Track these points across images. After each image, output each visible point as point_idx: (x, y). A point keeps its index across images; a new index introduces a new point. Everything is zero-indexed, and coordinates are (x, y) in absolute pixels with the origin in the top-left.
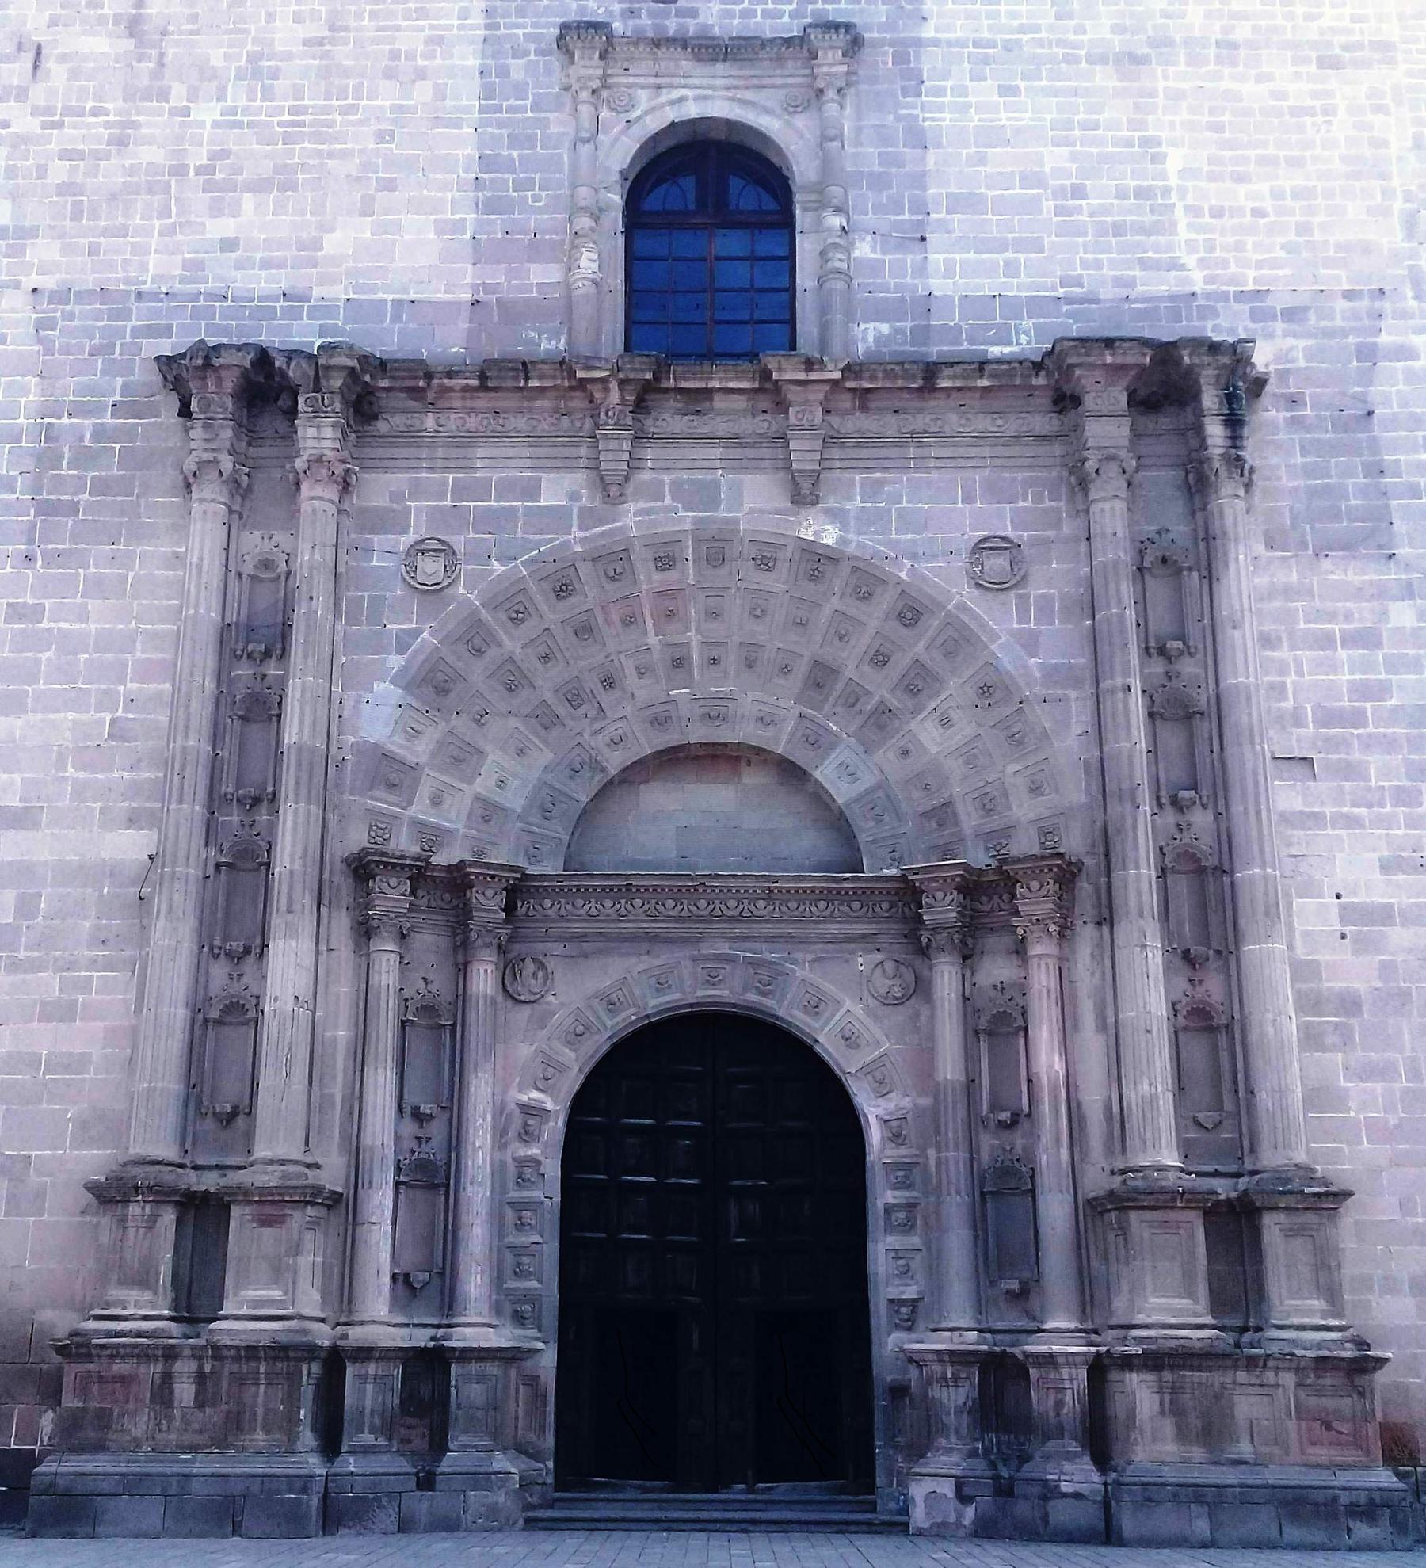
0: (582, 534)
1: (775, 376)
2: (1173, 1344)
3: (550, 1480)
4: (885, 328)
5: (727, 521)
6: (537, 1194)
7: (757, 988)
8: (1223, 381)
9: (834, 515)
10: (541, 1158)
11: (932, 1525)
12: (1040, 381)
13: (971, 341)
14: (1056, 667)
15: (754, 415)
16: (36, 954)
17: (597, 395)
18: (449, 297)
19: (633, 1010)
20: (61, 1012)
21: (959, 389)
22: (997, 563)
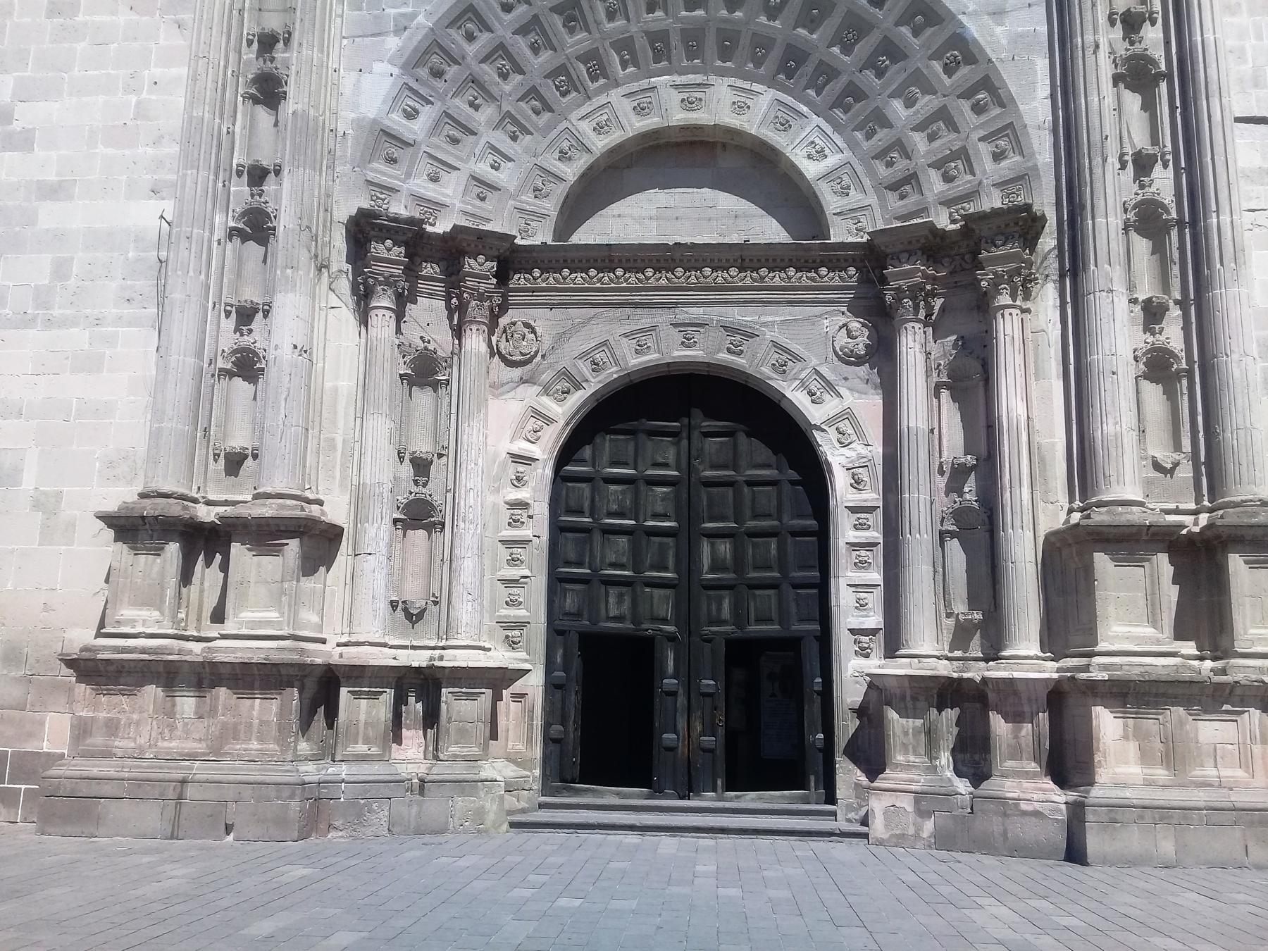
2: (1137, 671)
3: (537, 786)
6: (525, 532)
14: (1021, 35)
16: (68, 312)
19: (615, 369)
20: (89, 364)
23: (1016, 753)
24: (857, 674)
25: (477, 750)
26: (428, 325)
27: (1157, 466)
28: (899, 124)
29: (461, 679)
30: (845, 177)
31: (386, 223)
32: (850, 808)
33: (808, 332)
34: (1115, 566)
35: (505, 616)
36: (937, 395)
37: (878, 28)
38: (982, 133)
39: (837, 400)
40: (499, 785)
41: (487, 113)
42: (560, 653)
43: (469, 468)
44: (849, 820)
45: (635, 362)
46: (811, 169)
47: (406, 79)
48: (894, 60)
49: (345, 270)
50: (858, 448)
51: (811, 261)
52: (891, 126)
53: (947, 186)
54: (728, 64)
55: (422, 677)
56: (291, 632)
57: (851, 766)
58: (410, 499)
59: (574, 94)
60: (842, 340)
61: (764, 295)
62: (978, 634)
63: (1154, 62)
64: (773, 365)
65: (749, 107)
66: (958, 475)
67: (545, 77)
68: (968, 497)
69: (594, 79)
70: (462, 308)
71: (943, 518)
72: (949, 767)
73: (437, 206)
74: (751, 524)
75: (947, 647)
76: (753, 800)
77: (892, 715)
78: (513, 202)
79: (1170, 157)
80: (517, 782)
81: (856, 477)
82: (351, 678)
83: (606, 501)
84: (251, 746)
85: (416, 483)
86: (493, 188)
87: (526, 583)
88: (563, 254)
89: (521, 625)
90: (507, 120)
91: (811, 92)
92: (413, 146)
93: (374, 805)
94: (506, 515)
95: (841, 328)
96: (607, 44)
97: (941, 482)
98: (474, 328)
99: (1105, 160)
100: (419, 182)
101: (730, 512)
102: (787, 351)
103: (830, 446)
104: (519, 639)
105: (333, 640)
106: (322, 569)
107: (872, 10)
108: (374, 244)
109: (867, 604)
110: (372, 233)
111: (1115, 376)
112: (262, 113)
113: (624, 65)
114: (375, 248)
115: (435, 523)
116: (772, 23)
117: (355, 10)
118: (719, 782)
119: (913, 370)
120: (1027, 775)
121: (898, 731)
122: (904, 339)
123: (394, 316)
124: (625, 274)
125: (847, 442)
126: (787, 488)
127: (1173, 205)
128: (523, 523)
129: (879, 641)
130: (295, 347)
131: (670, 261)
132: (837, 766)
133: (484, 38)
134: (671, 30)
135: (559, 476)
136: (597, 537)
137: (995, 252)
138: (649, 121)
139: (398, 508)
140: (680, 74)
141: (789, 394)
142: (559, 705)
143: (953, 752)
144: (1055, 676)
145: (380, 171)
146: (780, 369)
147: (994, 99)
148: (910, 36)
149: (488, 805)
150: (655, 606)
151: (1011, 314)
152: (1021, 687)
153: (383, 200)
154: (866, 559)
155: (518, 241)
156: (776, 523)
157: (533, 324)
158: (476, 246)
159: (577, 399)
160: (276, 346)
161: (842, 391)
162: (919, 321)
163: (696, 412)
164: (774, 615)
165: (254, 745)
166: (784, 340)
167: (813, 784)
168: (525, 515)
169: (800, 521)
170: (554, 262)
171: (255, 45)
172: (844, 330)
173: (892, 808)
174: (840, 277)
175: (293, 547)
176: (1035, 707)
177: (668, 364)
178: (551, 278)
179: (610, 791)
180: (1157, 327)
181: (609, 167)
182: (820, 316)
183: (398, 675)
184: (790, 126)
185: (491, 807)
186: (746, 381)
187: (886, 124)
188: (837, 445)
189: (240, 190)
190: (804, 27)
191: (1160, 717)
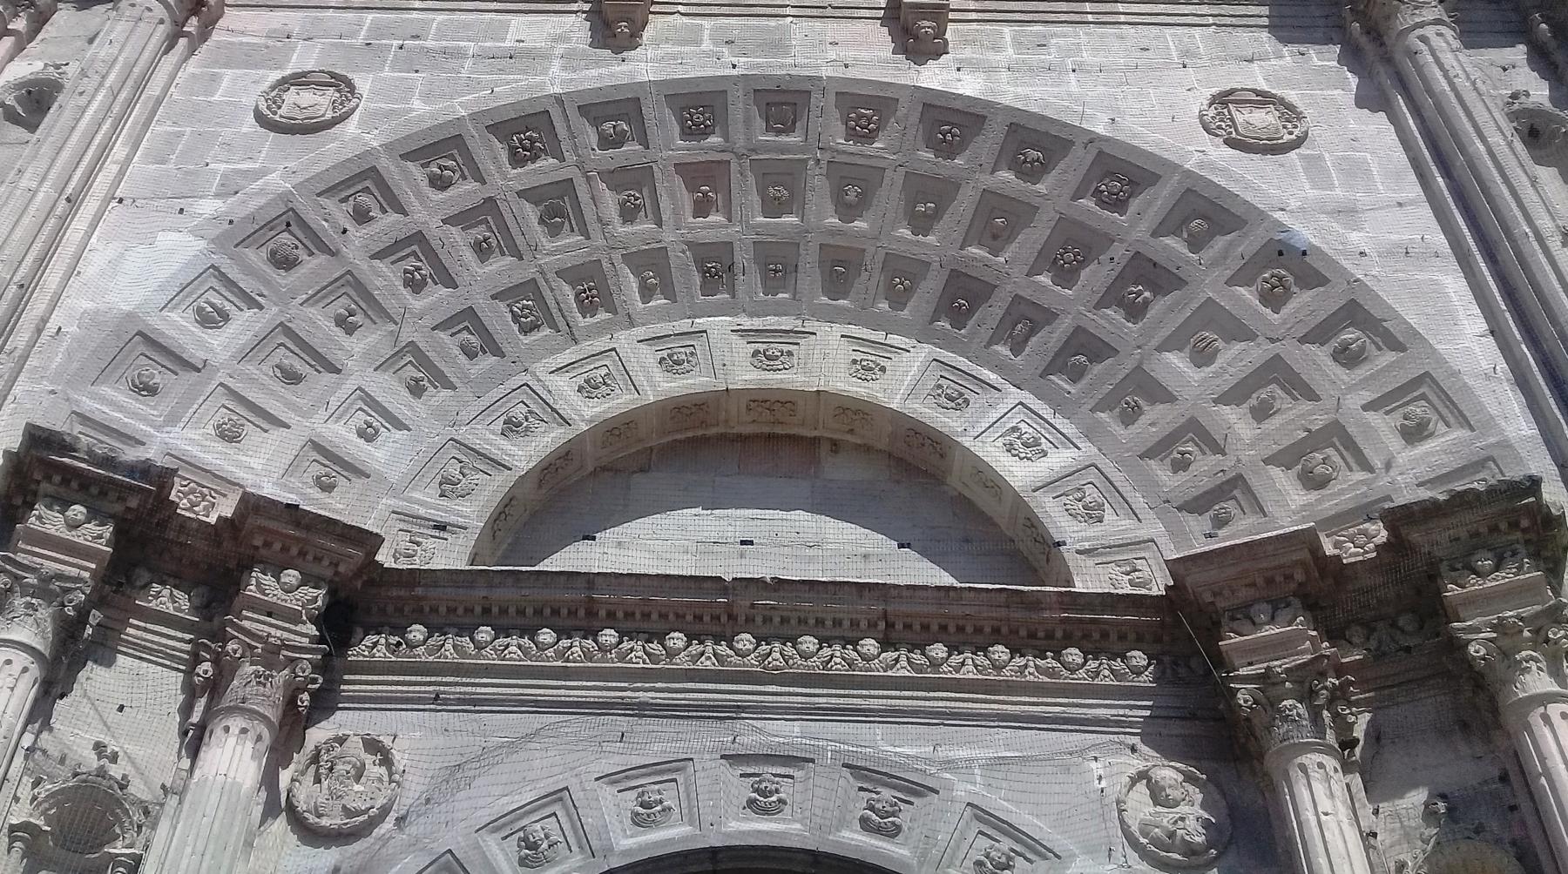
30: (1089, 489)
37: (1121, 241)
41: (369, 340)
46: (1018, 473)
48: (1159, 289)
51: (1041, 634)
59: (546, 331)
61: (940, 701)
65: (883, 369)
67: (494, 297)
69: (587, 308)
78: (391, 502)
86: (354, 470)
88: (483, 593)
90: (409, 358)
91: (1003, 350)
92: (199, 370)
96: (617, 256)
100: (191, 433)
113: (647, 293)
117: (151, 163)
124: (621, 642)
131: (724, 619)
133: (387, 224)
134: (737, 245)
140: (751, 315)
148: (1186, 251)
157: (387, 741)
170: (460, 611)
178: (448, 646)
181: (604, 469)
184: (967, 402)
187: (1160, 394)
190: (980, 244)
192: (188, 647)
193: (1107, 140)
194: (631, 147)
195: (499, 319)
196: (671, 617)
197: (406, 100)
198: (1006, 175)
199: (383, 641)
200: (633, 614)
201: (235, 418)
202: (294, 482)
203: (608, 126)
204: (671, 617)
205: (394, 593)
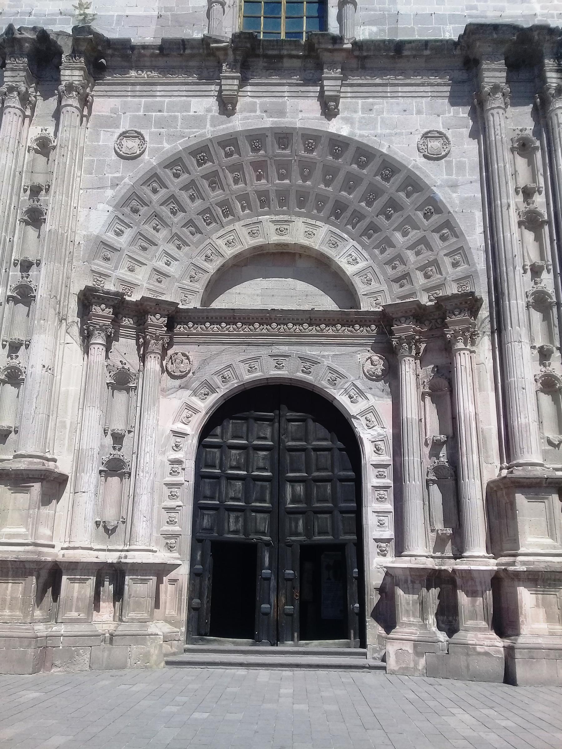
0: (212, 129)
1: (316, 46)
3: (183, 638)
4: (374, 29)
5: (291, 123)
6: (180, 479)
7: (302, 370)
8: (555, 51)
9: (347, 120)
10: (184, 460)
11: (400, 668)
12: (457, 52)
13: (419, 36)
14: (467, 199)
15: (305, 70)
17: (222, 57)
18: (145, 14)
19: (236, 381)
21: (414, 57)
22: (435, 145)
23: (473, 616)
24: (379, 567)
25: (146, 615)
26: (125, 354)
27: (550, 443)
28: (398, 246)
29: (137, 570)
30: (369, 274)
31: (102, 294)
32: (375, 651)
33: (348, 361)
34: (528, 502)
35: (166, 531)
36: (423, 399)
37: (387, 193)
38: (446, 252)
39: (366, 401)
40: (160, 638)
41: (163, 234)
42: (199, 553)
43: (147, 439)
44: (374, 658)
45: (248, 377)
46: (350, 270)
47: (117, 213)
48: (396, 211)
49: (76, 321)
50: (378, 429)
51: (350, 321)
52: (394, 247)
53: (426, 281)
54: (303, 210)
55: (114, 569)
56: (33, 541)
57: (376, 624)
58: (111, 457)
59: (214, 224)
60: (368, 366)
61: (323, 340)
62: (450, 542)
63: (541, 215)
64: (329, 380)
65: (314, 234)
66: (436, 446)
68: (442, 459)
69: (226, 216)
70: (146, 344)
71: (428, 472)
72: (434, 624)
73: (132, 286)
74: (316, 474)
75: (432, 550)
76: (316, 646)
77: (400, 592)
79: (551, 267)
80: (170, 636)
81: (377, 447)
82: (70, 569)
83: (229, 459)
84: (5, 613)
85: (114, 448)
86: (166, 275)
87: (179, 510)
89: (176, 536)
91: (349, 227)
93: (81, 651)
94: (168, 468)
95: (367, 360)
96: (234, 197)
97: (427, 450)
98: (153, 356)
99: (515, 268)
100: (122, 271)
101: (303, 467)
102: (337, 372)
103: (362, 428)
104: (175, 545)
105: (59, 544)
106: (54, 502)
107: (383, 182)
108: (94, 307)
109: (384, 524)
110: (93, 300)
111: (524, 390)
112: (31, 231)
113: (243, 209)
114: (95, 309)
115: (125, 473)
116: (327, 188)
118: (296, 635)
119: (409, 384)
120: (480, 630)
121: (403, 602)
122: (403, 367)
123: (104, 349)
125: (372, 426)
126: (337, 452)
127: (554, 294)
128: (179, 473)
129: (392, 547)
130: (44, 366)
131: (269, 319)
132: (367, 624)
133: (163, 192)
135: (202, 445)
136: (224, 482)
137: (454, 318)
138: (257, 241)
139: (103, 463)
140: (276, 215)
141: (337, 397)
142: (198, 587)
143: (437, 615)
144: (495, 568)
145: (100, 265)
146: (333, 382)
147: (452, 233)
149: (152, 651)
150: (258, 524)
151: (464, 354)
152: (475, 575)
153: (101, 281)
154: (384, 496)
155: (180, 306)
156: (330, 473)
157: (188, 354)
158: (155, 309)
159: (213, 398)
160: (32, 365)
161: (369, 396)
162: (412, 356)
163: (284, 407)
164: (329, 530)
165: (7, 612)
166: (334, 366)
167: (352, 635)
168: (180, 468)
169: (345, 473)
171: (28, 192)
172: (369, 361)
173: (400, 651)
174: (366, 330)
175: (36, 487)
176: (484, 588)
177: (267, 378)
178: (199, 328)
179: (228, 641)
180: (547, 362)
181: (234, 265)
182: (356, 352)
183: (99, 568)
184: (338, 245)
185: (154, 652)
186: (313, 389)
187: (391, 245)
188: (366, 427)
189: (15, 274)
190: (345, 191)
191: (557, 593)
192: (135, 333)
193: (386, 155)
194: (235, 156)
195: (200, 223)
196: (255, 319)
197: (161, 143)
198: (355, 166)
199: (182, 327)
200: (245, 318)
201: (132, 264)
202: (151, 281)
203: (227, 148)
204: (255, 319)
205: (183, 314)
